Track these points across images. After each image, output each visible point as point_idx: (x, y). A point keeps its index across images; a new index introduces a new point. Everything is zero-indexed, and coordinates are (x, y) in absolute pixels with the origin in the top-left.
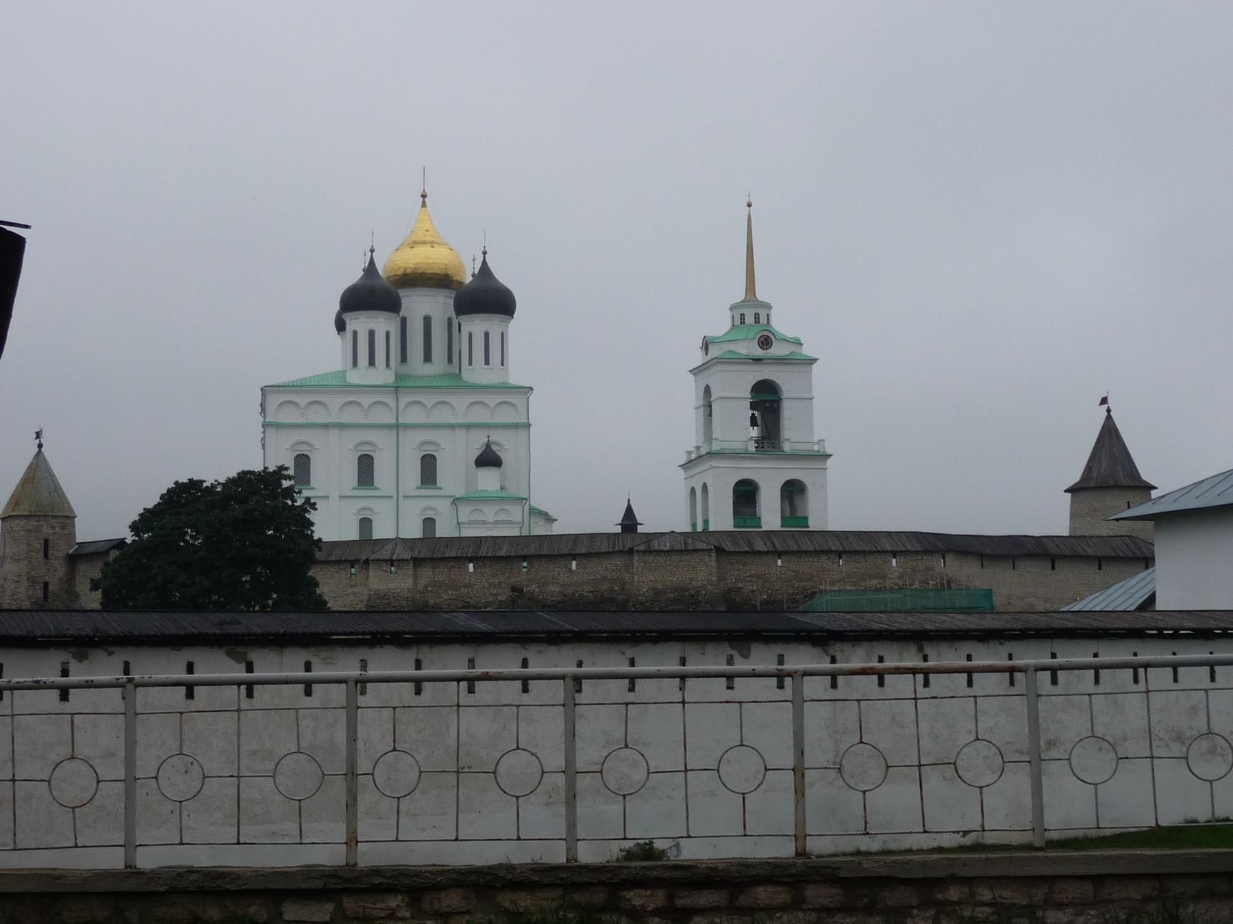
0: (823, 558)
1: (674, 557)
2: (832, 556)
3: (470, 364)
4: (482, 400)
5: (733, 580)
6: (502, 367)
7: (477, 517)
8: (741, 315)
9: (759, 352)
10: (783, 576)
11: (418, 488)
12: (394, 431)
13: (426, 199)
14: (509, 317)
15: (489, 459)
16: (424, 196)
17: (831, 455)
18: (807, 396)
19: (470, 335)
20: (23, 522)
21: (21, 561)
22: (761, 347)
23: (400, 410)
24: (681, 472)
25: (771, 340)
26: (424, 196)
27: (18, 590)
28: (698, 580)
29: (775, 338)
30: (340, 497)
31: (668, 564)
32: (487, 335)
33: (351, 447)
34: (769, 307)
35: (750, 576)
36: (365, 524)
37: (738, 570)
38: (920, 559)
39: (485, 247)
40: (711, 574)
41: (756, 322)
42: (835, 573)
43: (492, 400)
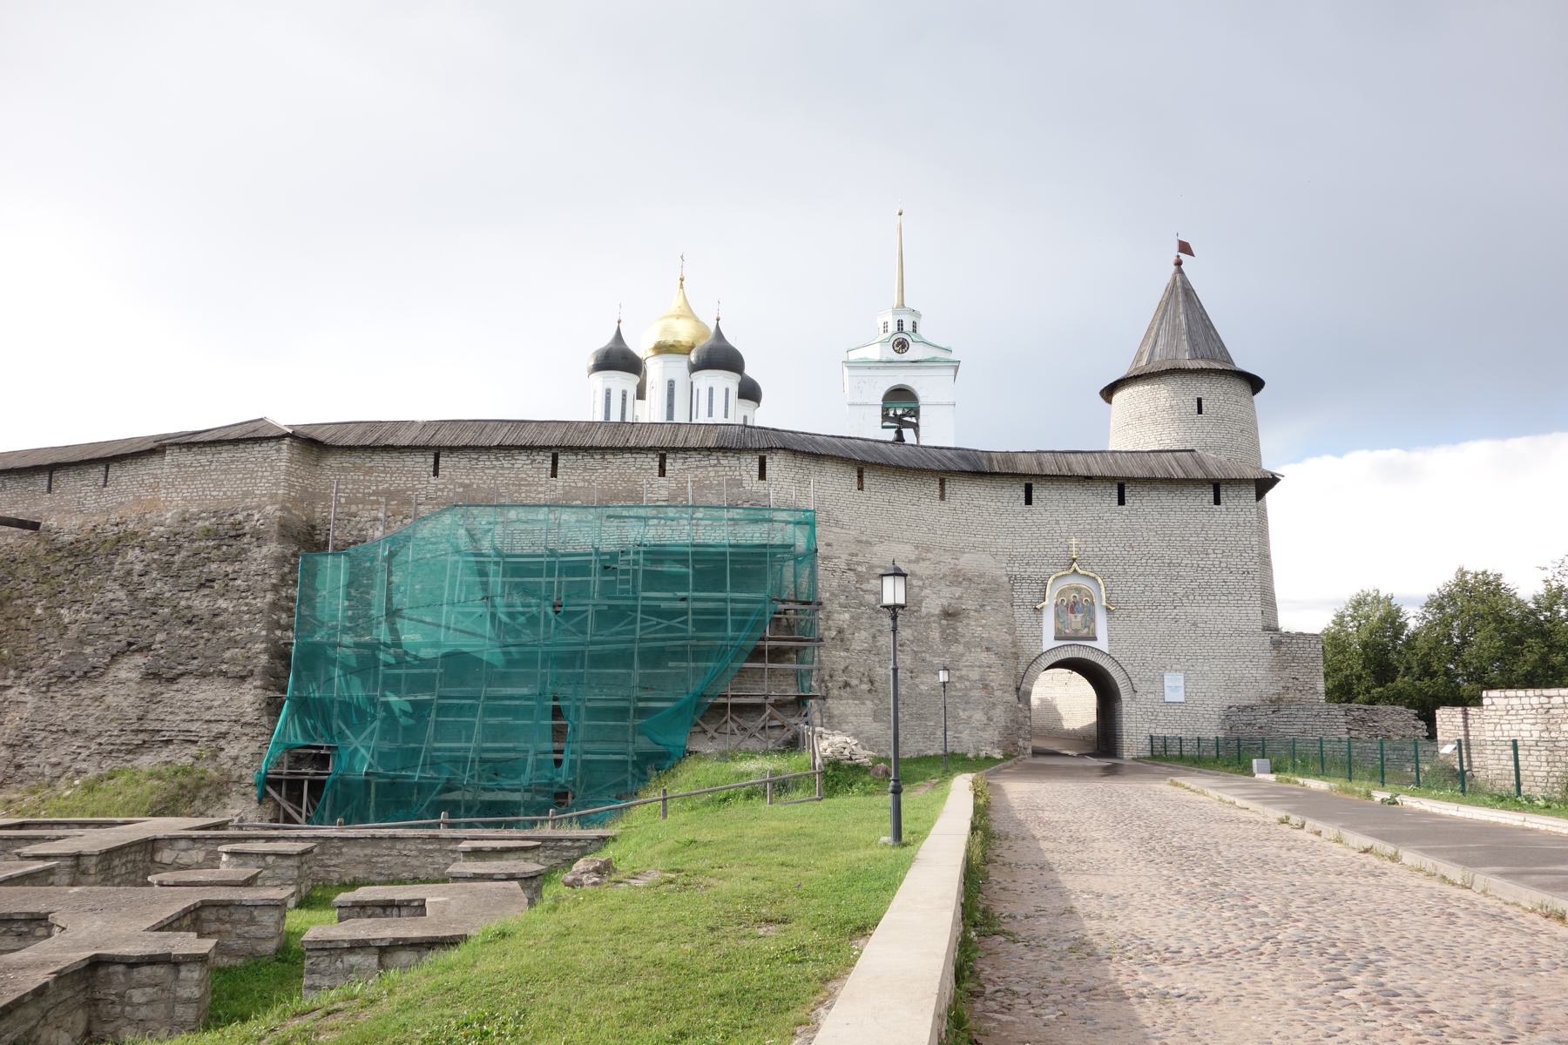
0: (522, 460)
1: (225, 455)
2: (539, 458)
5: (343, 500)
9: (896, 357)
10: (439, 493)
16: (682, 280)
26: (682, 280)
28: (256, 495)
31: (213, 467)
32: (711, 390)
35: (374, 493)
37: (354, 482)
38: (715, 466)
40: (276, 484)
42: (540, 489)
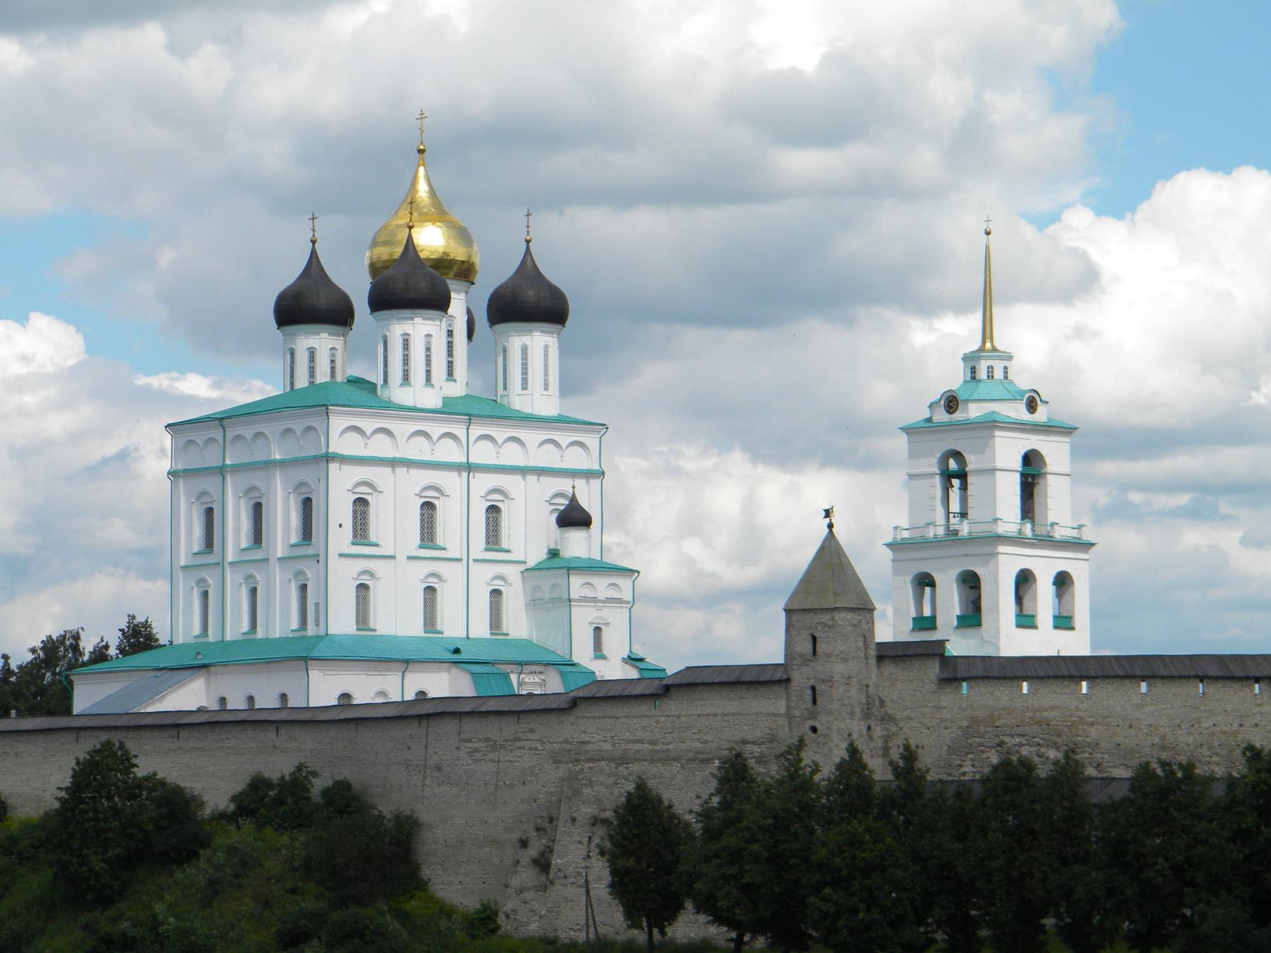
3: (525, 386)
8: (988, 368)
12: (465, 474)
14: (559, 327)
15: (573, 517)
17: (1093, 544)
18: (988, 466)
19: (525, 350)
20: (850, 616)
21: (850, 661)
24: (889, 554)
27: (849, 694)
33: (482, 495)
34: (1010, 358)
43: (564, 438)
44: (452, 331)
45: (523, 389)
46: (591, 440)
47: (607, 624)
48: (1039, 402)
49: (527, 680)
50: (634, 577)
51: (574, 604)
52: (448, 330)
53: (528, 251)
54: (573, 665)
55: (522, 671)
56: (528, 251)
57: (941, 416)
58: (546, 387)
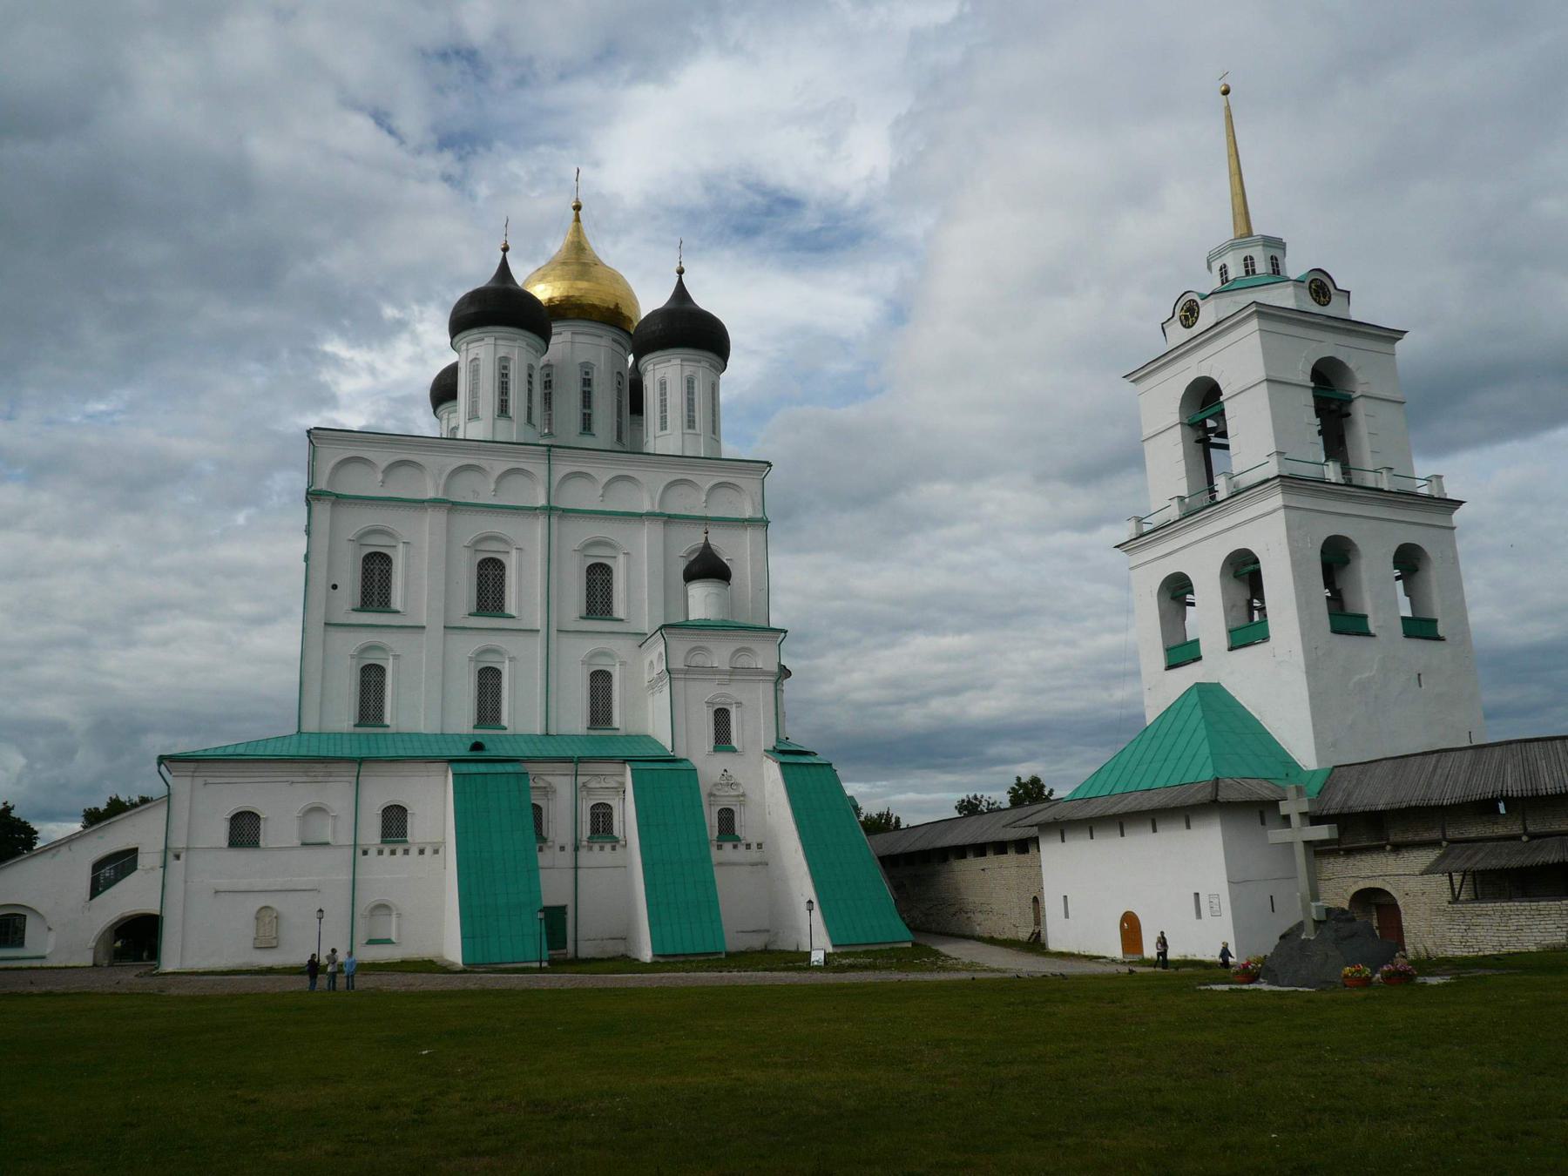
3: (664, 426)
4: (689, 477)
6: (713, 436)
7: (698, 660)
8: (1246, 259)
11: (581, 618)
13: (580, 212)
15: (708, 567)
19: (663, 385)
22: (1315, 300)
23: (555, 484)
25: (1328, 290)
26: (578, 208)
29: (1335, 288)
30: (445, 627)
32: (690, 383)
36: (489, 681)
39: (680, 263)
41: (1274, 270)
43: (707, 480)
44: (589, 380)
45: (662, 429)
46: (748, 483)
47: (739, 704)
48: (1332, 290)
49: (593, 784)
50: (778, 642)
51: (680, 676)
52: (584, 379)
53: (680, 281)
54: (673, 760)
55: (577, 771)
56: (680, 281)
57: (1178, 334)
58: (691, 423)
